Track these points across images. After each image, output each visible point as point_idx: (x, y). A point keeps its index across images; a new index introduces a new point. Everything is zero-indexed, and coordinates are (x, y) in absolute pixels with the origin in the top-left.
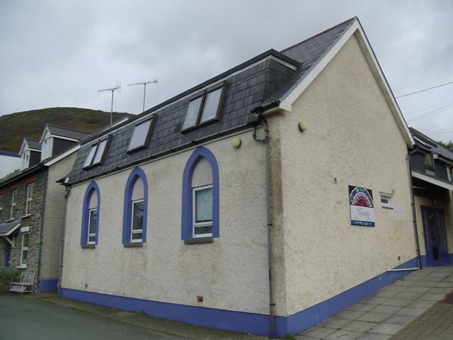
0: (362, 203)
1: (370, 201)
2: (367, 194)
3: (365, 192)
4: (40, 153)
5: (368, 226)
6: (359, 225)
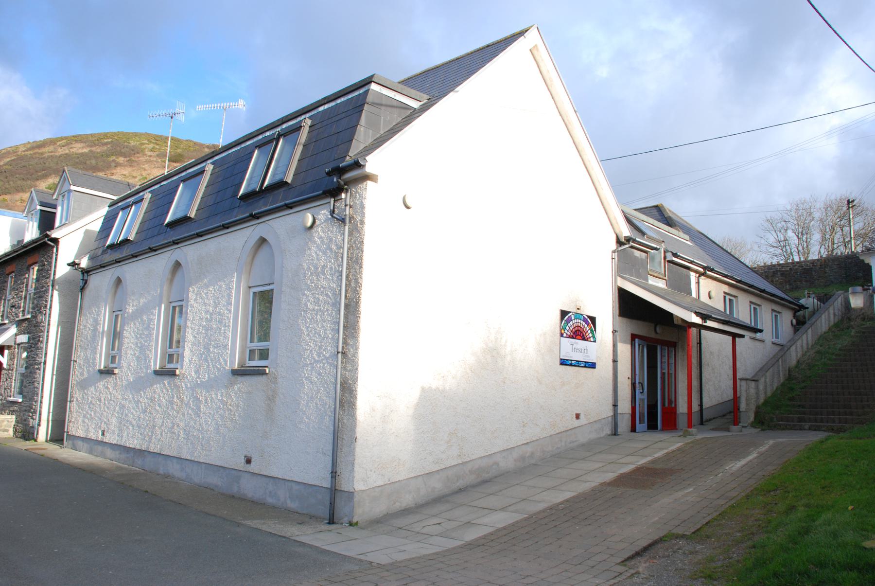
0: (578, 334)
1: (592, 332)
2: (588, 324)
3: (585, 320)
4: (55, 213)
5: (585, 367)
6: (571, 365)
